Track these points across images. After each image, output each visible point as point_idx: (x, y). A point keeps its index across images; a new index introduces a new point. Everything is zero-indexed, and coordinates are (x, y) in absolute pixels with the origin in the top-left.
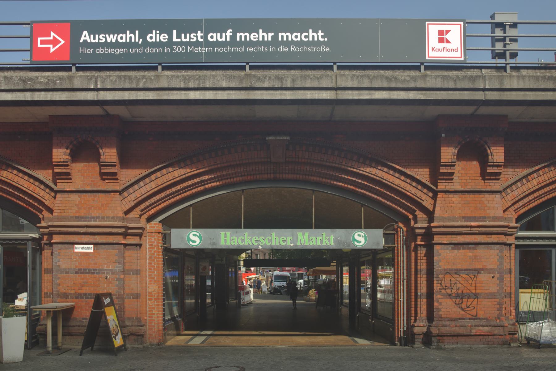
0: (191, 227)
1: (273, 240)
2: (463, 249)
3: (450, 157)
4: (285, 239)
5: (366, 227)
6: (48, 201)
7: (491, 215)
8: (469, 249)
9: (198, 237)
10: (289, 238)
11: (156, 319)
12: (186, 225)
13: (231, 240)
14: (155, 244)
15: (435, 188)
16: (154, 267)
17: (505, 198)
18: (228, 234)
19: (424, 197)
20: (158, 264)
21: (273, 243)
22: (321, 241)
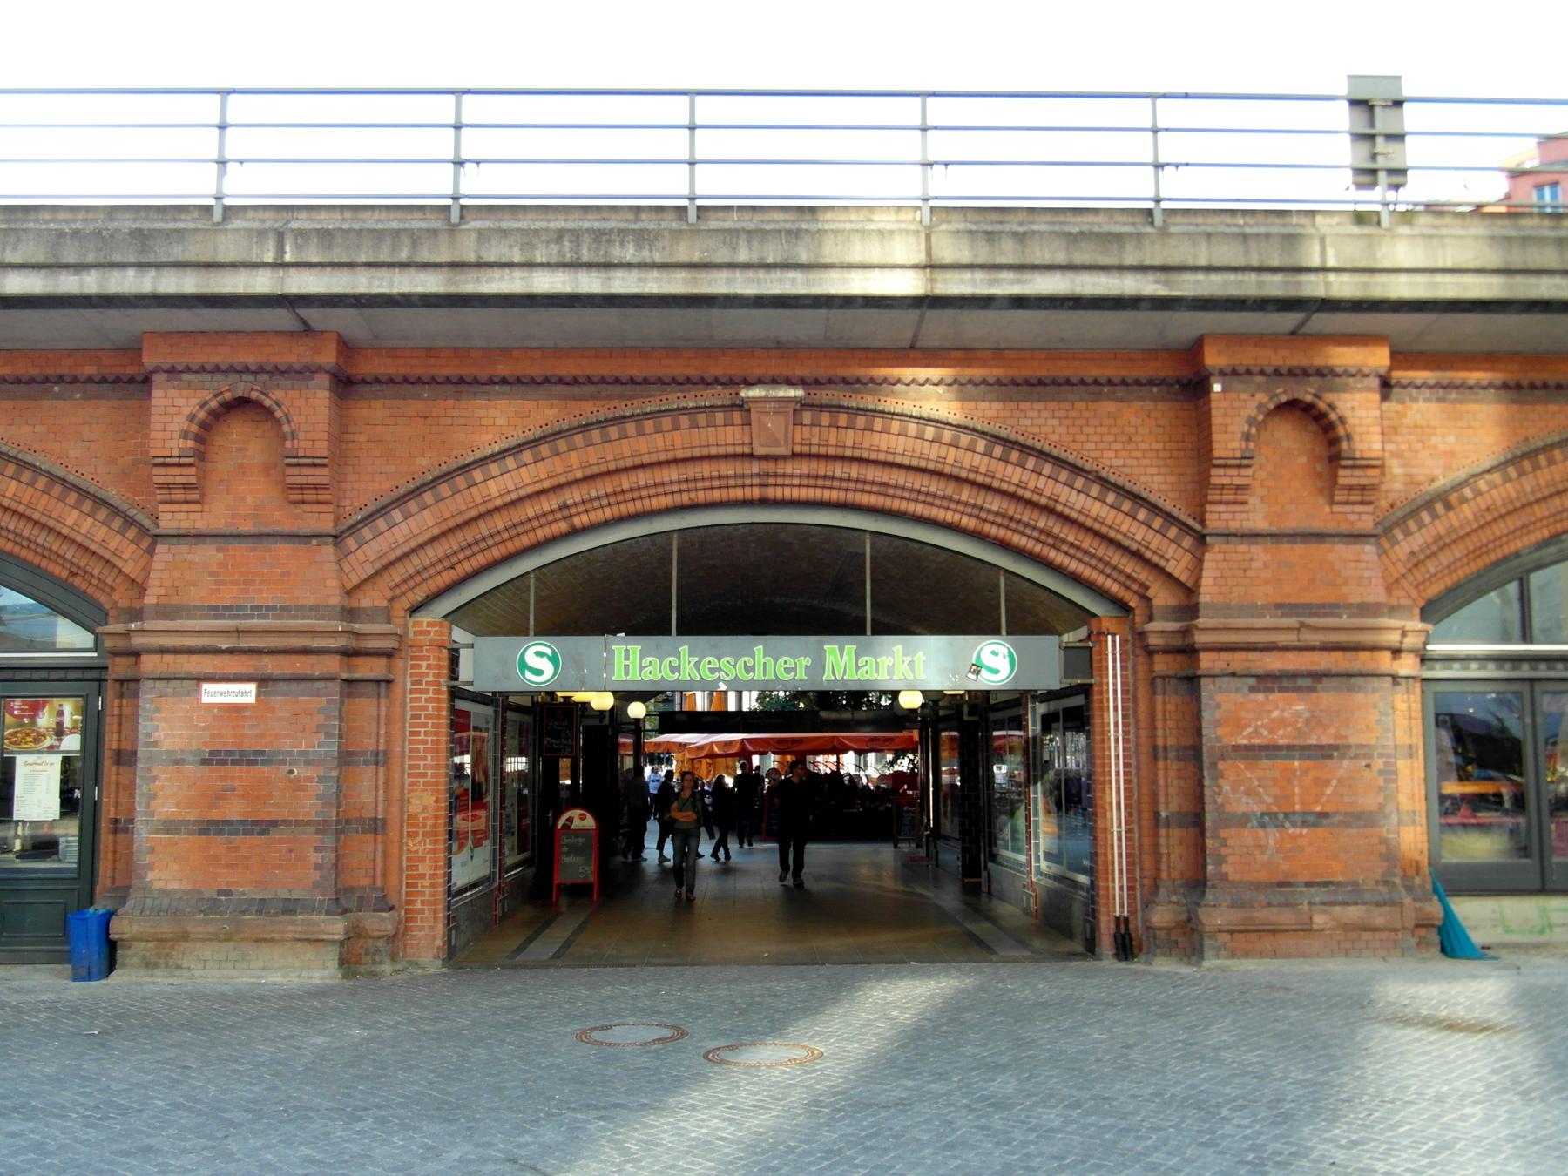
1: (759, 670)
2: (1281, 690)
3: (1235, 444)
6: (131, 564)
7: (1355, 600)
8: (1299, 690)
9: (550, 659)
10: (805, 661)
11: (427, 891)
12: (518, 629)
13: (641, 668)
14: (431, 679)
15: (1197, 527)
16: (425, 742)
17: (1390, 553)
19: (1171, 550)
20: (436, 734)
22: (891, 670)
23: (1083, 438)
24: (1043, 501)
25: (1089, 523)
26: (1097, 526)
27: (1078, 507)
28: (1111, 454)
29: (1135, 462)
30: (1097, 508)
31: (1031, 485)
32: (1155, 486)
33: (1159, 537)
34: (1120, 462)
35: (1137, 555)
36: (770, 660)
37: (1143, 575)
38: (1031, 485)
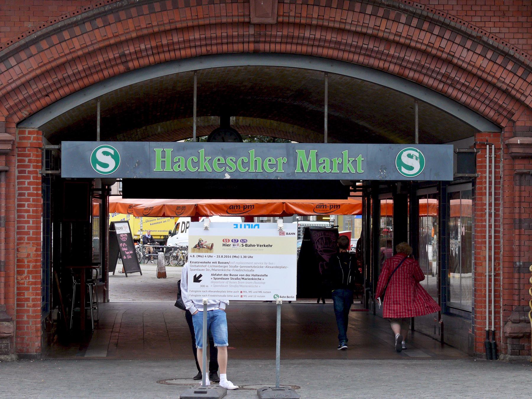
4: (273, 162)
5: (422, 142)
9: (113, 157)
11: (31, 309)
13: (173, 163)
14: (31, 169)
16: (28, 211)
18: (169, 151)
20: (35, 206)
21: (252, 169)
22: (341, 166)
23: (473, 13)
24: (444, 56)
25: (475, 71)
26: (479, 73)
27: (467, 60)
28: (491, 25)
29: (507, 30)
30: (481, 62)
31: (437, 45)
32: (520, 47)
33: (521, 81)
34: (497, 30)
35: (506, 93)
37: (509, 105)
38: (437, 45)
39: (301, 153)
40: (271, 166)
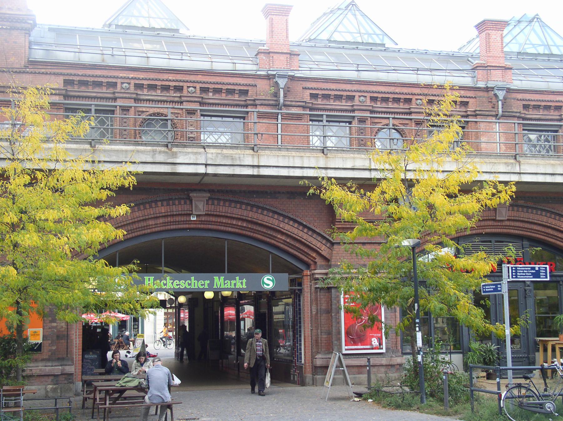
0: (226, 271)
1: (193, 284)
10: (207, 282)
18: (152, 278)
19: (323, 247)
21: (193, 287)
22: (235, 285)
36: (196, 282)
39: (216, 278)
40: (202, 285)
